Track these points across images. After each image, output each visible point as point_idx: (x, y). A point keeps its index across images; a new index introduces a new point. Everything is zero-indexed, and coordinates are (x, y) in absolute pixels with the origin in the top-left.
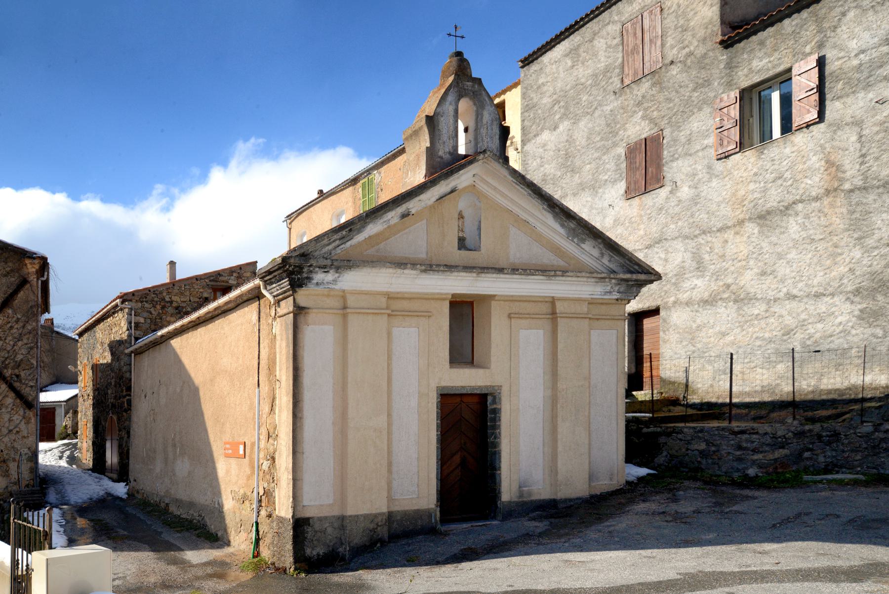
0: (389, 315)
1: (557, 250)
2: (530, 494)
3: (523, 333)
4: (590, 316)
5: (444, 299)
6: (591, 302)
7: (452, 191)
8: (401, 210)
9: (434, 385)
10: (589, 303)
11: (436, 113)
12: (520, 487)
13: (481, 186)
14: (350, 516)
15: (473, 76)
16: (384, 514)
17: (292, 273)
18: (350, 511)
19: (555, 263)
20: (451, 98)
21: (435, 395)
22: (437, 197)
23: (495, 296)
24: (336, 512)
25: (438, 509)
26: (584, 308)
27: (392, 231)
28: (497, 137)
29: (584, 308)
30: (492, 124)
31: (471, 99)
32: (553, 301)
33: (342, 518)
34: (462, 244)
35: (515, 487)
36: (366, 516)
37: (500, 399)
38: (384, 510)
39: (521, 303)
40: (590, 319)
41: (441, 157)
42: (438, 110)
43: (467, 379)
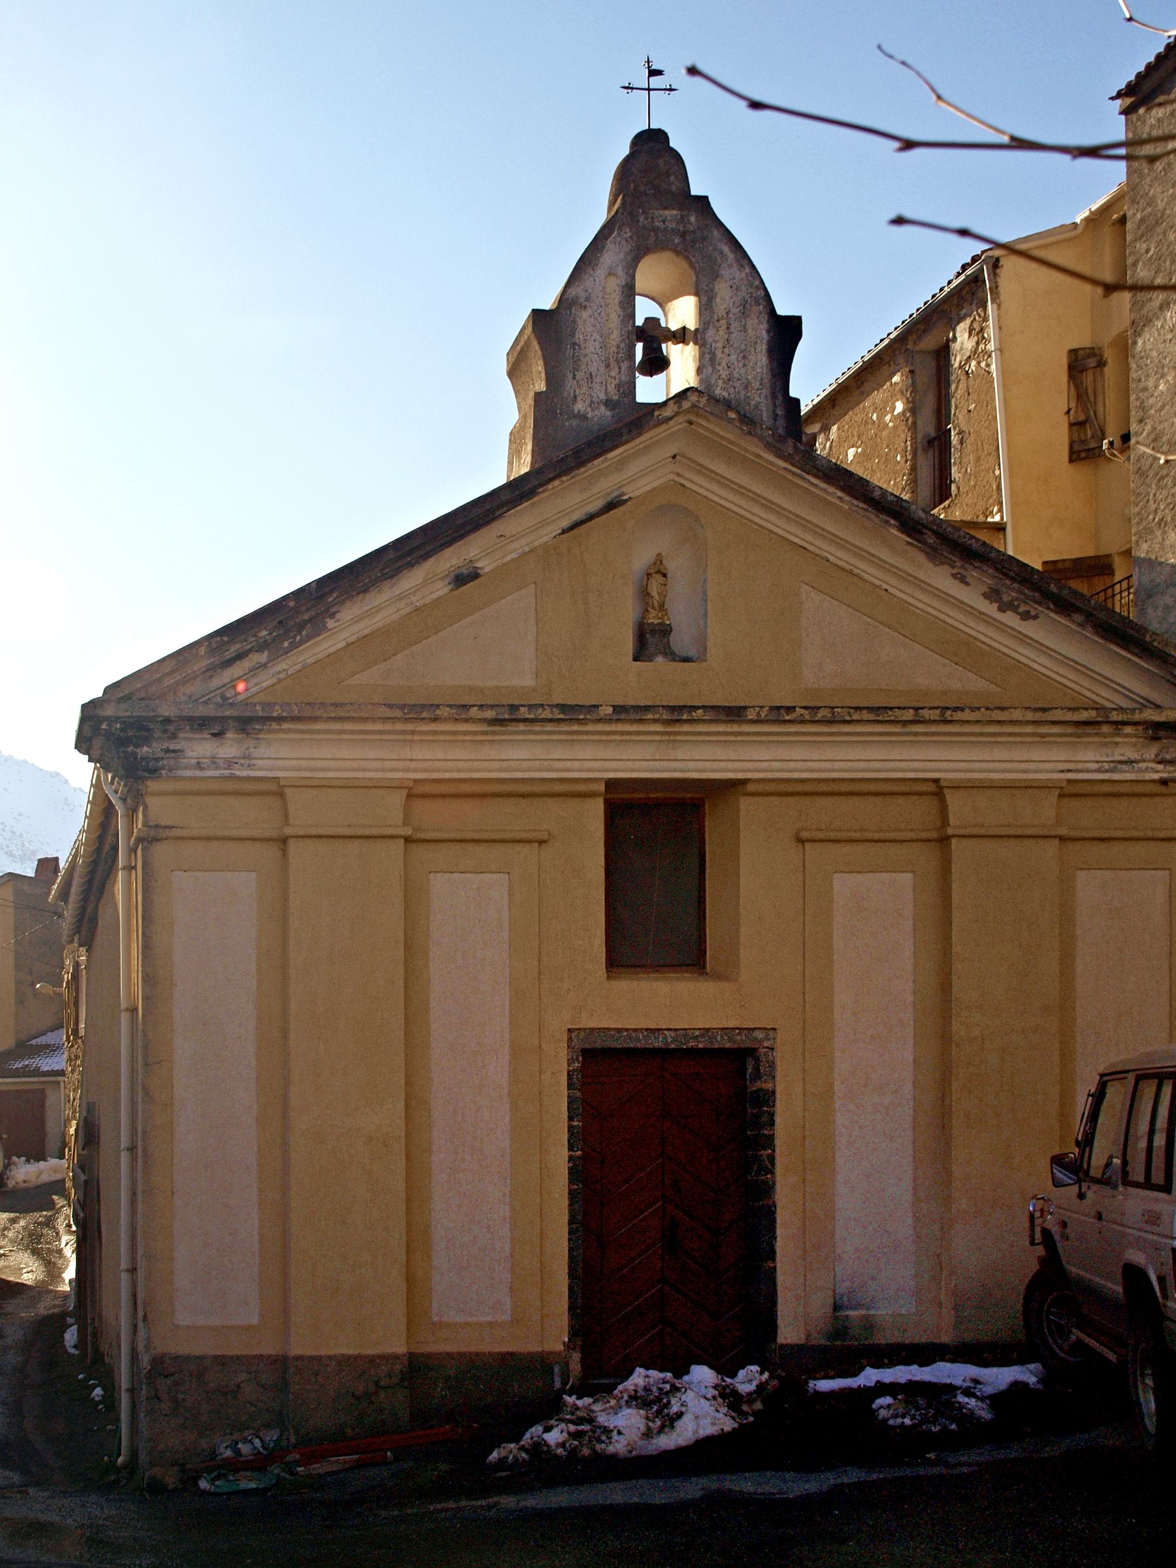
0: (407, 840)
1: (965, 652)
2: (869, 1325)
3: (844, 886)
4: (1063, 831)
5: (592, 795)
6: (1072, 792)
7: (611, 506)
8: (450, 559)
9: (558, 1023)
10: (1061, 796)
11: (565, 300)
12: (837, 1307)
13: (699, 484)
14: (298, 1358)
15: (693, 193)
16: (396, 1357)
17: (123, 742)
18: (301, 1346)
19: (955, 685)
20: (612, 256)
21: (563, 1055)
22: (565, 523)
23: (745, 782)
24: (269, 1348)
25: (576, 1356)
26: (1047, 810)
27: (422, 623)
28: (763, 347)
29: (1047, 810)
30: (744, 314)
31: (677, 253)
32: (937, 790)
33: (281, 1362)
34: (650, 640)
35: (819, 1306)
36: (344, 1362)
37: (772, 1065)
38: (399, 1347)
39: (1046, 833)
40: (1062, 839)
41: (582, 417)
42: (573, 292)
43: (663, 1007)
